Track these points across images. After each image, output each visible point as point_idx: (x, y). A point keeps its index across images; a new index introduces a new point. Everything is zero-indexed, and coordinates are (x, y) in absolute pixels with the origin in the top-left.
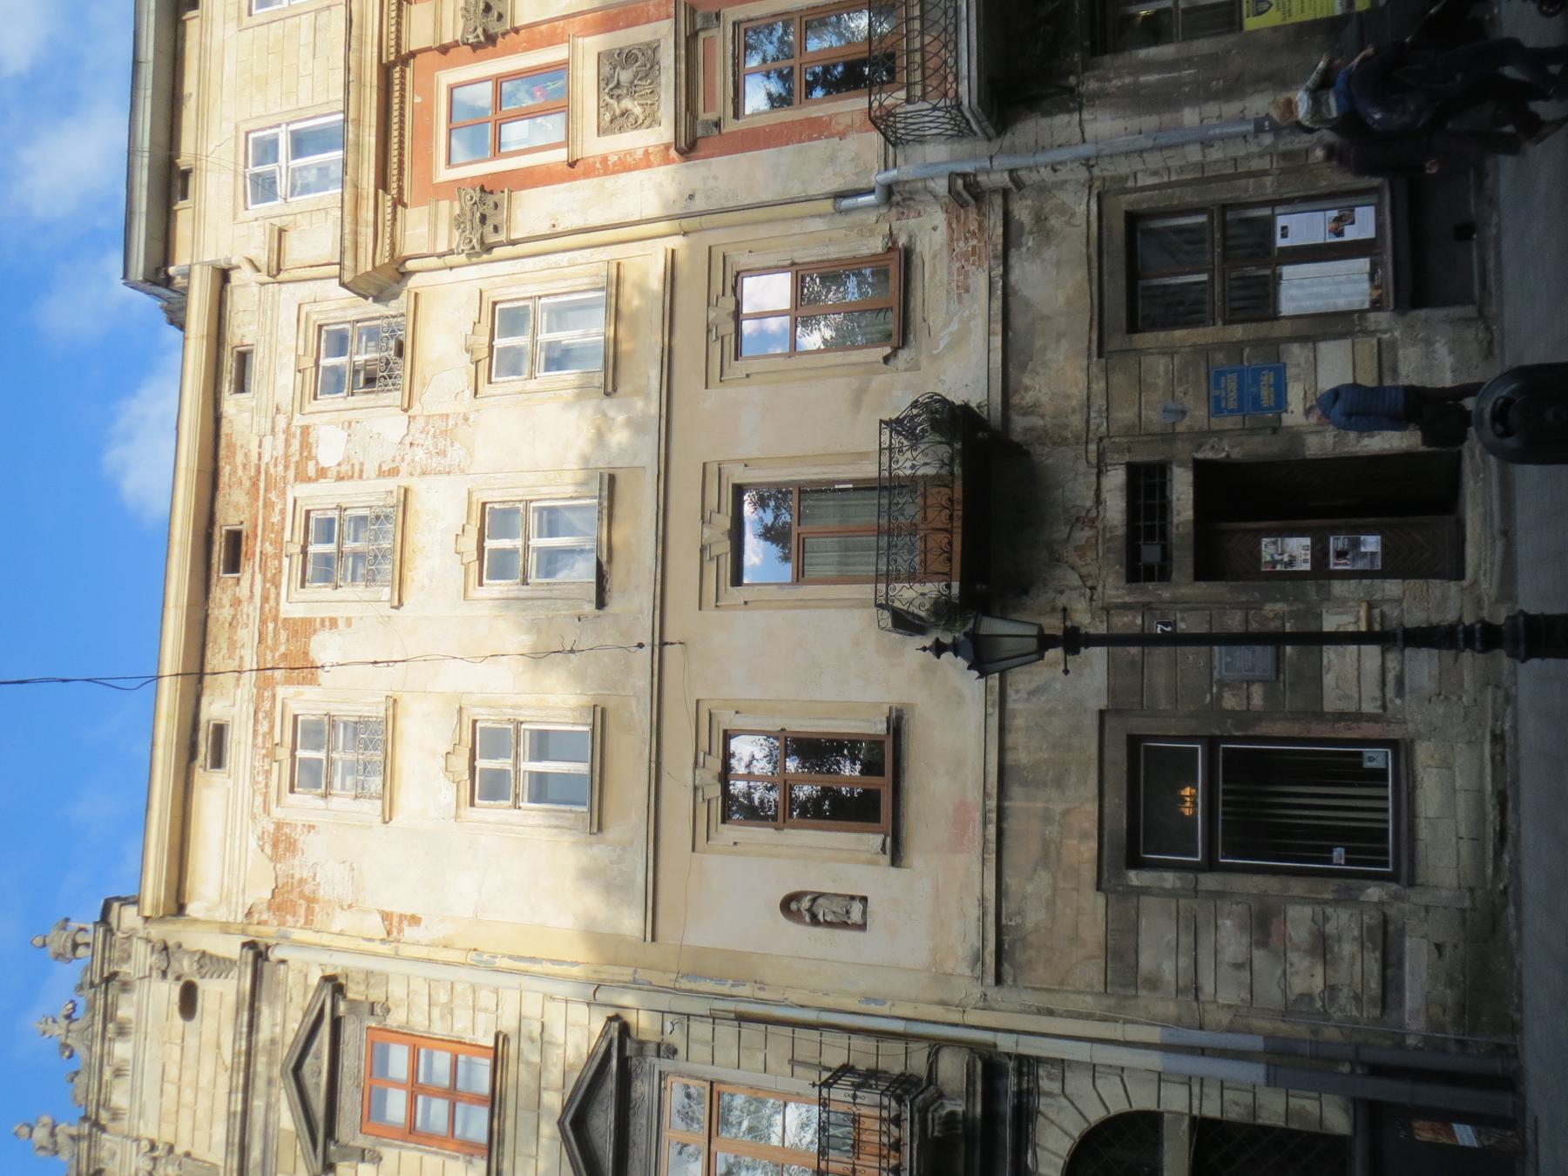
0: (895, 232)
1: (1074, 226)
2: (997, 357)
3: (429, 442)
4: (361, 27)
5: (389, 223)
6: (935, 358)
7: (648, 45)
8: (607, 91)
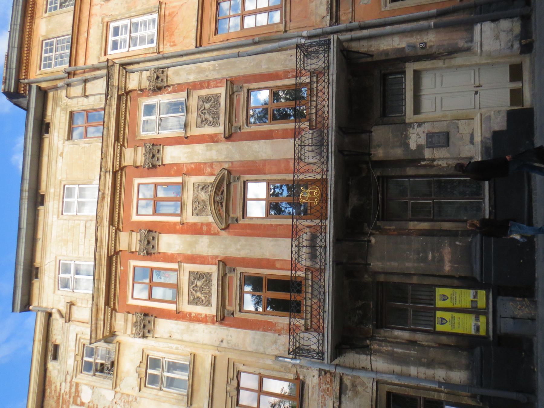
0: (298, 372)
1: (366, 392)
4: (101, 242)
5: (109, 319)
7: (208, 273)
8: (192, 287)
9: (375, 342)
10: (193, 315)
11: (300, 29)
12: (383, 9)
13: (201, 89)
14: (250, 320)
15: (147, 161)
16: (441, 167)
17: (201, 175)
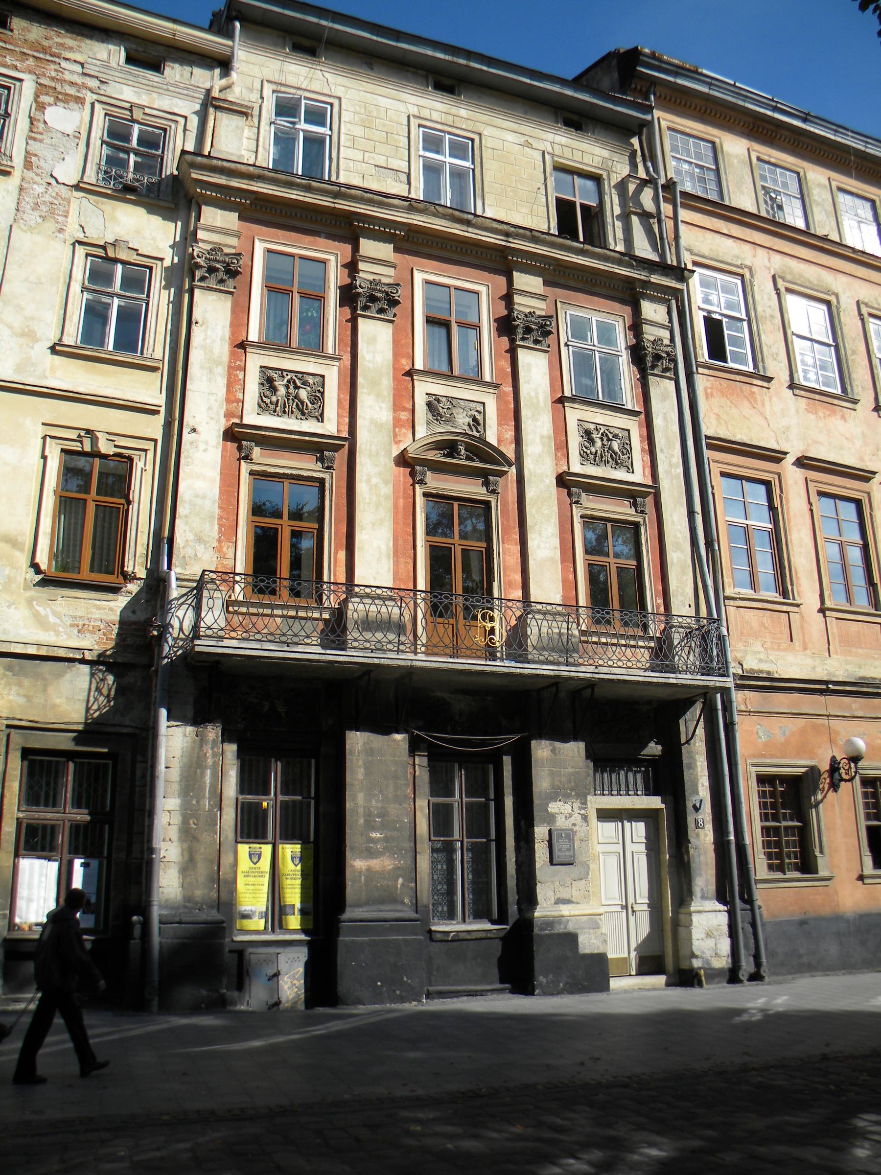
2: (19, 649)
3: (47, 198)
6: (30, 602)
8: (294, 377)
9: (220, 734)
12: (749, 761)
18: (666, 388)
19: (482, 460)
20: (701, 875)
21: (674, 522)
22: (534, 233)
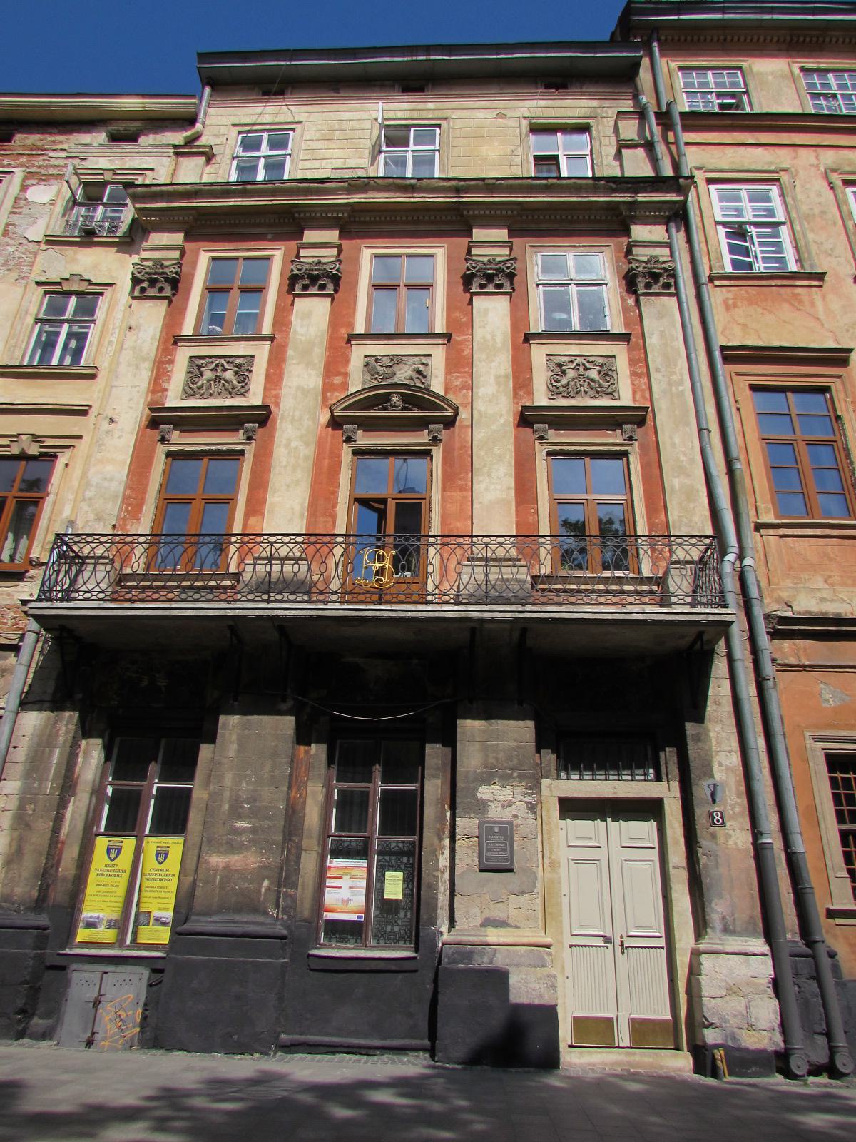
3: (18, 254)
7: (247, 391)
10: (169, 368)
11: (762, 557)
12: (807, 734)
13: (630, 360)
14: (149, 472)
15: (480, 265)
16: (437, 853)
17: (446, 368)
18: (664, 305)
19: (422, 409)
20: (720, 896)
21: (675, 444)
22: (486, 181)
